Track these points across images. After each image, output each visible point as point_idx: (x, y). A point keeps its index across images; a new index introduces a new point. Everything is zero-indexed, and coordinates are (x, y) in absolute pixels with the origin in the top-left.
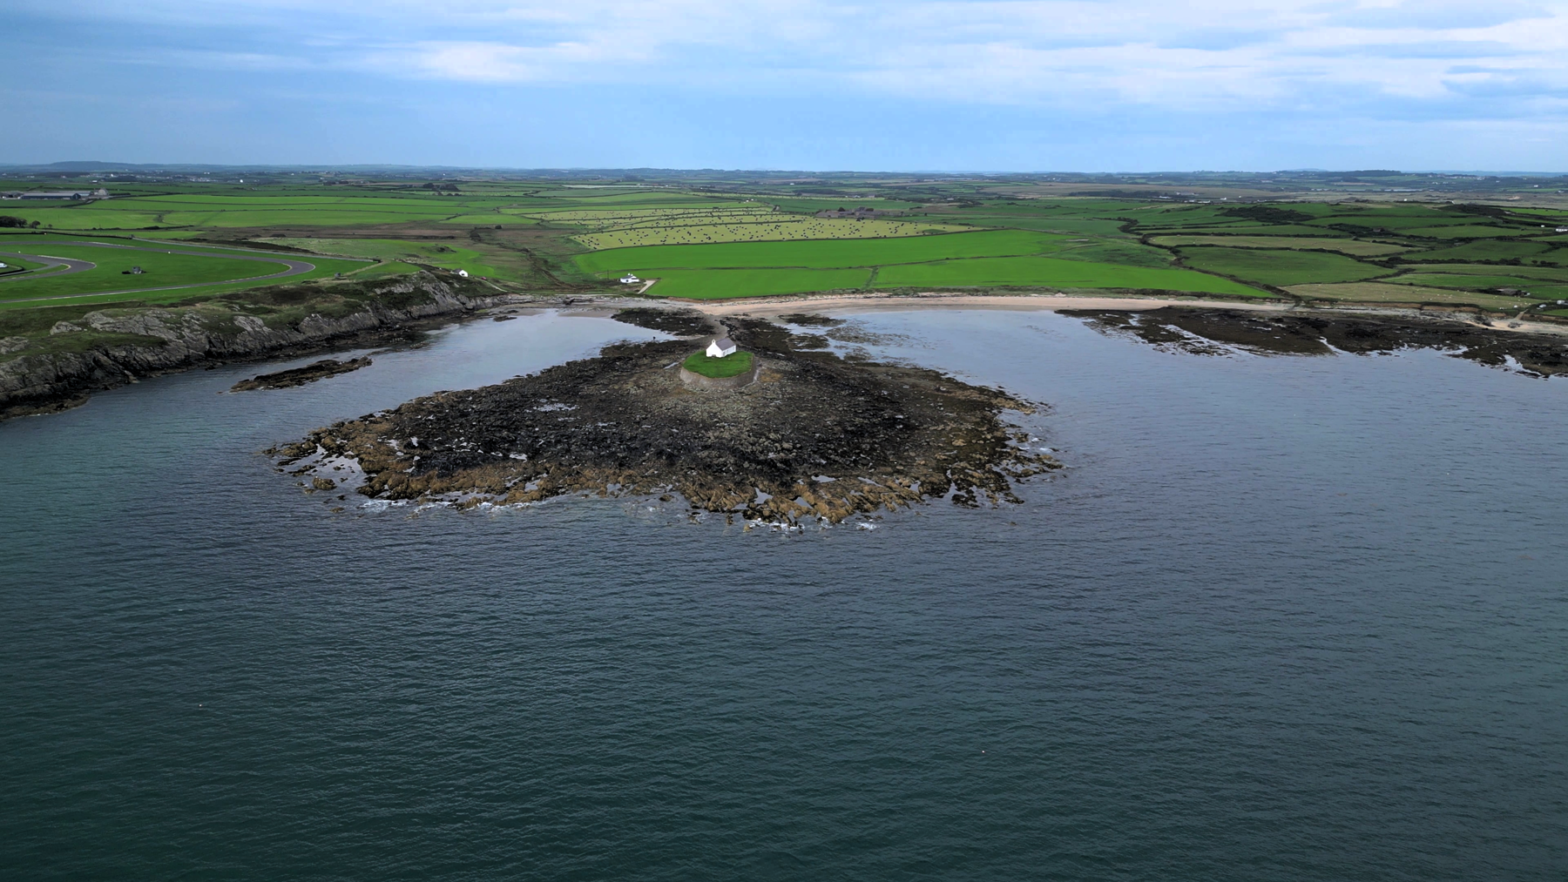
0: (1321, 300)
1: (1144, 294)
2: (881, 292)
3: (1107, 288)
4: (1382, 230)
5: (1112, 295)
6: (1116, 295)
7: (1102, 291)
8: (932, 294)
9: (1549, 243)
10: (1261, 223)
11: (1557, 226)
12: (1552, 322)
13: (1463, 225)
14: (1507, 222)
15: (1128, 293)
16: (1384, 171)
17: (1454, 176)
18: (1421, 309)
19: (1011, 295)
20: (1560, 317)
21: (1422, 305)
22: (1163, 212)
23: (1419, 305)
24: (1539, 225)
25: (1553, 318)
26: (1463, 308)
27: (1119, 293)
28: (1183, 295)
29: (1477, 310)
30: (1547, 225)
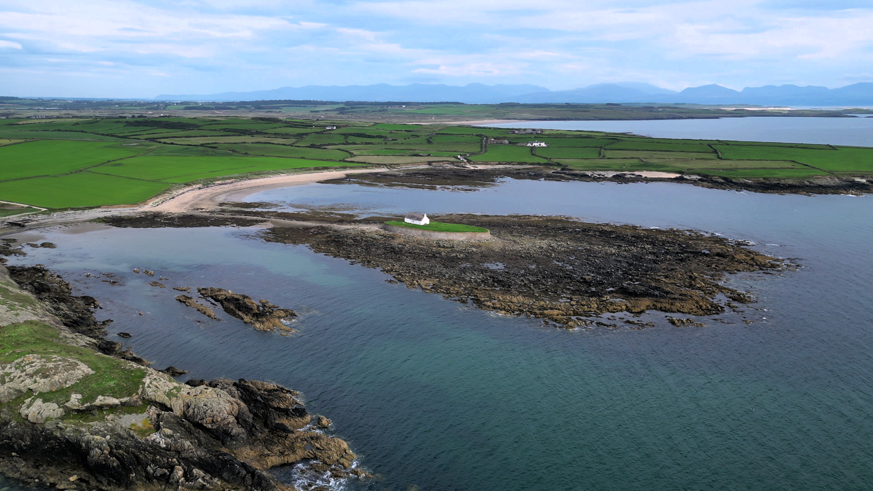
0: (394, 164)
3: (298, 169)
4: (256, 131)
9: (342, 134)
10: (181, 130)
11: (326, 127)
12: (482, 164)
14: (296, 125)
15: (311, 170)
16: (13, 97)
17: (54, 100)
18: (430, 165)
21: (430, 163)
22: (73, 125)
23: (427, 163)
24: (312, 126)
26: (444, 162)
27: (306, 170)
28: (336, 168)
29: (450, 163)
30: (315, 126)
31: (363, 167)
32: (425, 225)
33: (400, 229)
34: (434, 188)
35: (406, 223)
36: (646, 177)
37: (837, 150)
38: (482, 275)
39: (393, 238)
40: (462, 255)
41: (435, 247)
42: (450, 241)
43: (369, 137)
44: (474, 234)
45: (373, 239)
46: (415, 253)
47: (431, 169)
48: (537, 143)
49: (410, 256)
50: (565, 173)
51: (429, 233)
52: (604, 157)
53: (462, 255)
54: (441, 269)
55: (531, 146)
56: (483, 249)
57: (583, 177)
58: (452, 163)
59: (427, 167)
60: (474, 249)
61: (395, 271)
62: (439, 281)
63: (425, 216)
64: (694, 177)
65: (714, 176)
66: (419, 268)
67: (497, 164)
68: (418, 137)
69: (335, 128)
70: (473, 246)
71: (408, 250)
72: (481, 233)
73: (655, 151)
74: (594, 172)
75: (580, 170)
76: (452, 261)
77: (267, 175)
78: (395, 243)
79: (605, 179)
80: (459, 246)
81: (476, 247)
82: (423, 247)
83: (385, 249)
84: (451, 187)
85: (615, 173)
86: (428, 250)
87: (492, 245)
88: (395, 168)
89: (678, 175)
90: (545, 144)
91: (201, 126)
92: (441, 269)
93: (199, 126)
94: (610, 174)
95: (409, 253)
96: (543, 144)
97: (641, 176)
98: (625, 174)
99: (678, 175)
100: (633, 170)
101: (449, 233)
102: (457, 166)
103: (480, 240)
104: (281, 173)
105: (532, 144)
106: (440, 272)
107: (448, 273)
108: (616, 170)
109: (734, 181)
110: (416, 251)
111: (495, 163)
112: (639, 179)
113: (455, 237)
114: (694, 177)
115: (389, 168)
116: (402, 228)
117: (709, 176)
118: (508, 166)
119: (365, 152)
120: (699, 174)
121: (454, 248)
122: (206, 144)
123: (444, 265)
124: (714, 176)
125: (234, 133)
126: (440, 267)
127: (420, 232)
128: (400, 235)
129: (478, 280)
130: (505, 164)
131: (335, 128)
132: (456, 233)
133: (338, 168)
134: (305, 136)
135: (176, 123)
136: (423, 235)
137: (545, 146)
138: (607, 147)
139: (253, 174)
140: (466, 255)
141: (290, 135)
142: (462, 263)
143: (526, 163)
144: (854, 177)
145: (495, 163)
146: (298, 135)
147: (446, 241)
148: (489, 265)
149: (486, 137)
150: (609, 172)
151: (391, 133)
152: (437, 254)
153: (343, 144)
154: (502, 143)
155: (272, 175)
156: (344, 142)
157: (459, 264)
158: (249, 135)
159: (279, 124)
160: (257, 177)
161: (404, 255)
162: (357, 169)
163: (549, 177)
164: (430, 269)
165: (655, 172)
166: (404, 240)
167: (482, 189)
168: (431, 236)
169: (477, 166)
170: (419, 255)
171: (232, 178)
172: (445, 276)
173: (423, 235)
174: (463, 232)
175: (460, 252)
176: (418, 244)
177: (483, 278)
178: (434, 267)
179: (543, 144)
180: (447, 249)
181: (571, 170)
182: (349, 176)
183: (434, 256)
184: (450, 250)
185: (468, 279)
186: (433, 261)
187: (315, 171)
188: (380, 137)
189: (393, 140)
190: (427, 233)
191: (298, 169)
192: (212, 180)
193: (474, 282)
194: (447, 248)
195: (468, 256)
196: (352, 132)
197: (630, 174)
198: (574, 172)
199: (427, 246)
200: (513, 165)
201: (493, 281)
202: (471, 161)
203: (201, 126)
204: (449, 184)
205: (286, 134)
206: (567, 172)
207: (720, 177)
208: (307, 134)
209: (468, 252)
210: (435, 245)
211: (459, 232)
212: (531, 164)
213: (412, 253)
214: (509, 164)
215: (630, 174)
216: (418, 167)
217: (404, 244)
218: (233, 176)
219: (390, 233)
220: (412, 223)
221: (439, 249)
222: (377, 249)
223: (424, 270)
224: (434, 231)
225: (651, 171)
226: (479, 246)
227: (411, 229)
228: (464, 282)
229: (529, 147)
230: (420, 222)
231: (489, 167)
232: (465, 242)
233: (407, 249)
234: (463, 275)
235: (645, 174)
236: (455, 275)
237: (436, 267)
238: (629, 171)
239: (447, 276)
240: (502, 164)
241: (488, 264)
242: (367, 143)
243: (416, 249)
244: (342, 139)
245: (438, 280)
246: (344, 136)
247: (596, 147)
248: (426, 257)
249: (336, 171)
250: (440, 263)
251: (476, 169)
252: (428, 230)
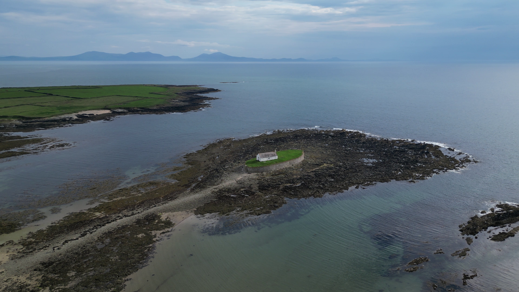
33: (275, 166)
37: (102, 88)
57: (65, 122)
97: (93, 114)
120: (120, 108)
136: (290, 164)
144: (172, 100)
168: (295, 162)
181: (40, 118)
206: (33, 120)
220: (269, 160)
225: (86, 110)
235: (95, 112)
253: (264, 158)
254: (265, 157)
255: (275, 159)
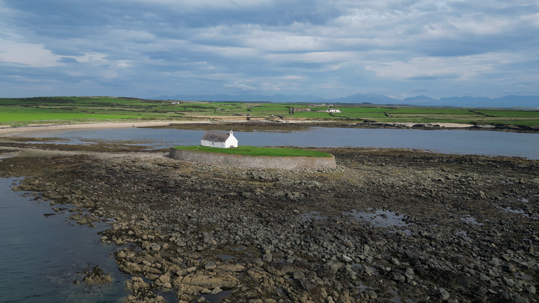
1: (145, 120)
2: (3, 125)
3: (126, 118)
4: (117, 104)
5: (132, 121)
6: (135, 121)
7: (126, 120)
8: (36, 125)
9: (183, 106)
13: (138, 102)
18: (249, 120)
19: (85, 123)
20: (295, 118)
25: (292, 119)
26: (260, 118)
27: (134, 120)
28: (163, 119)
31: (188, 120)
32: (232, 148)
33: (191, 154)
34: (252, 131)
35: (203, 146)
36: (443, 127)
38: (367, 247)
39: (176, 167)
40: (297, 194)
41: (243, 180)
42: (269, 170)
43: (204, 108)
44: (310, 160)
45: (143, 169)
46: (203, 190)
47: (250, 122)
48: (333, 109)
49: (190, 197)
50: (368, 124)
51: (236, 159)
52: (392, 117)
53: (297, 194)
54: (253, 227)
55: (328, 112)
56: (333, 183)
58: (268, 119)
59: (246, 121)
60: (318, 184)
61: (134, 236)
62: (245, 273)
63: (231, 135)
64: (489, 126)
65: (509, 124)
66: (198, 224)
67: (305, 120)
68: (241, 108)
69: (179, 103)
70: (312, 178)
71: (192, 185)
72: (322, 158)
73: (430, 114)
74: (395, 123)
75: (382, 122)
76: (278, 207)
77: (92, 122)
78: (175, 175)
79: (408, 128)
80: (287, 178)
81: (317, 180)
82: (222, 180)
83: (150, 184)
84: (268, 131)
85: (415, 124)
86: (229, 184)
87: (345, 176)
88: (217, 121)
89: (473, 126)
90: (339, 111)
91: (76, 101)
92: (253, 227)
93: (74, 101)
94: (411, 125)
95: (192, 191)
96: (338, 111)
97: (439, 126)
98: (424, 125)
99: (473, 126)
100: (428, 122)
101: (269, 158)
102: (272, 120)
103: (321, 169)
104: (107, 121)
105: (329, 111)
106: (248, 238)
107: (270, 242)
108: (414, 122)
109: (532, 127)
110: (205, 187)
111: (304, 119)
112: (437, 127)
113: (278, 164)
114: (489, 126)
115: (211, 121)
116: (194, 152)
117: (504, 124)
118: (315, 121)
119: (196, 114)
120: (492, 124)
121: (277, 180)
122: (66, 108)
123: (260, 215)
124: (509, 124)
125: (98, 105)
126: (250, 221)
127: (222, 157)
128: (190, 164)
129: (370, 271)
130: (313, 120)
131: (179, 103)
132: (281, 158)
133: (164, 119)
134: (154, 107)
135: (57, 99)
136: (226, 162)
137: (340, 112)
138: (390, 112)
139: (77, 121)
140: (306, 195)
141: (142, 107)
142: (301, 212)
143: (330, 119)
145: (304, 119)
146: (148, 106)
147: (264, 171)
148: (367, 216)
149: (292, 107)
150: (407, 123)
151: (221, 105)
152: (247, 191)
153: (182, 111)
154: (305, 111)
155: (97, 122)
156: (184, 110)
157: (295, 214)
158: (110, 106)
159: (136, 101)
160: (80, 123)
161: (178, 195)
162: (182, 121)
163: (353, 126)
164: (225, 228)
165: (448, 123)
166: (192, 170)
167: (297, 132)
168: (239, 163)
169: (289, 121)
170: (209, 195)
171: (51, 122)
172: (262, 251)
173: (226, 162)
174: (292, 156)
175: (293, 189)
176: (215, 176)
177: (376, 259)
178: (235, 222)
179: (338, 111)
180: (265, 184)
181: (373, 122)
182: (171, 125)
183: (240, 196)
184: (271, 184)
185: (336, 266)
186: (237, 207)
187: (142, 121)
188: (212, 108)
189: (221, 110)
190: (232, 158)
191: (126, 118)
192: (26, 122)
193: (358, 277)
194: (265, 181)
195: (310, 196)
196: (191, 105)
197: (427, 125)
198: (376, 123)
199: (230, 178)
200: (319, 120)
201: (416, 272)
202: (284, 117)
203: (76, 101)
204: (266, 129)
205: (139, 106)
206: (370, 123)
207: (516, 125)
208: (155, 106)
209: (308, 189)
210: (245, 177)
211: (286, 156)
212: (335, 120)
213: (197, 191)
214: (316, 120)
215: (427, 125)
216: (238, 121)
217: (189, 175)
218: (53, 120)
219: (176, 161)
220: (212, 146)
221: (251, 182)
222: (135, 183)
223: (209, 230)
224: (244, 155)
225: (445, 122)
226: (322, 179)
227: (207, 153)
228: (327, 281)
229: (327, 112)
230: (223, 143)
231: (299, 122)
232: (297, 173)
233: (191, 183)
234: (314, 246)
235: (441, 125)
236: (292, 247)
237: (240, 220)
238: (425, 123)
239: (268, 249)
240: (310, 120)
241: (361, 214)
242: (200, 111)
243: (207, 183)
244: (183, 109)
245: (240, 267)
246: (184, 108)
247: (381, 112)
248: (224, 197)
249: (162, 121)
250: (252, 211)
251: (288, 122)
252: (234, 154)
253: (205, 139)
254: (207, 140)
255: (222, 147)
